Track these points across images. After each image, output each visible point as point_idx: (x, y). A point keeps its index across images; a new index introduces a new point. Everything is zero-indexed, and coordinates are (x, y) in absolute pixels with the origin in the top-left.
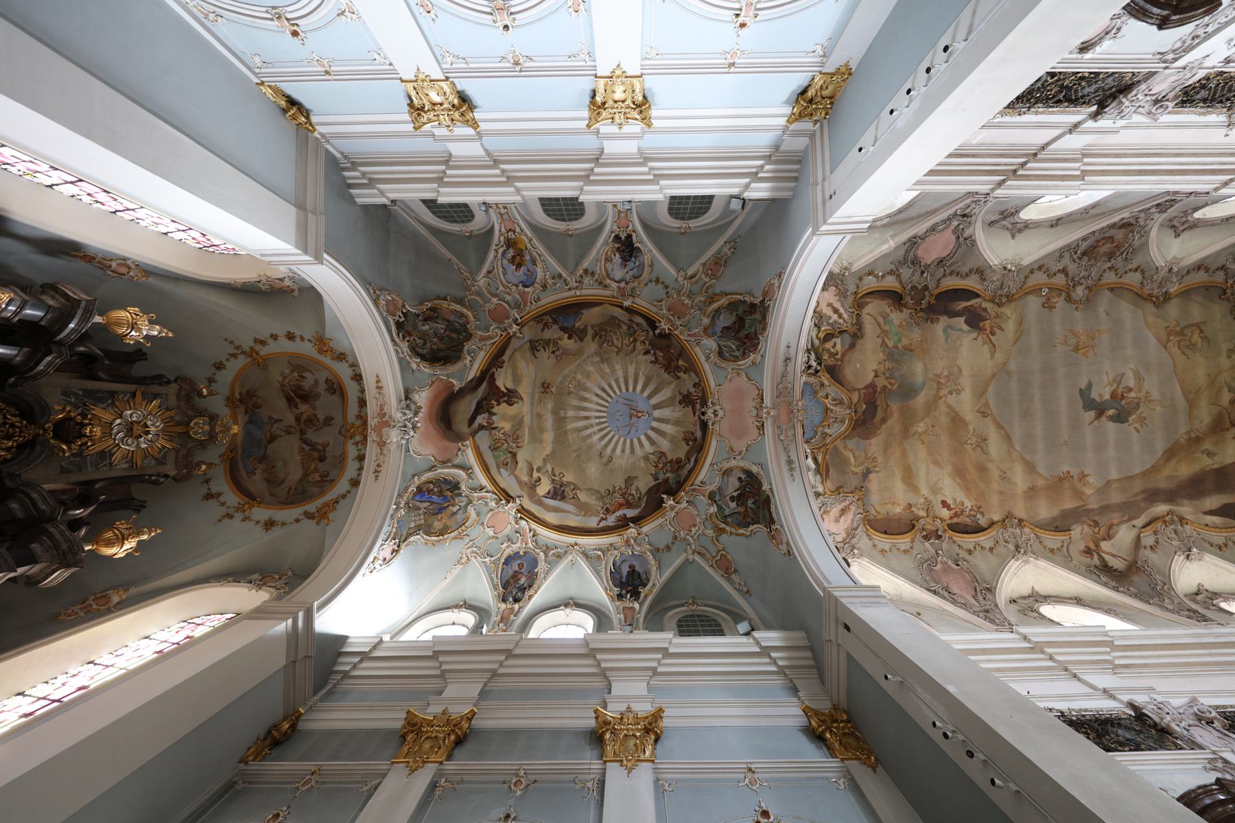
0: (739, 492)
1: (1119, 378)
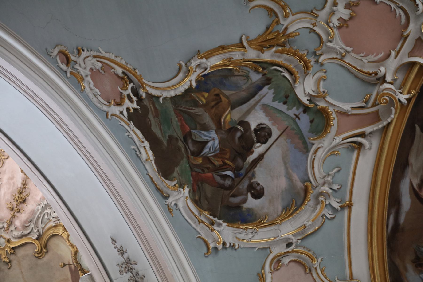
0: (251, 158)
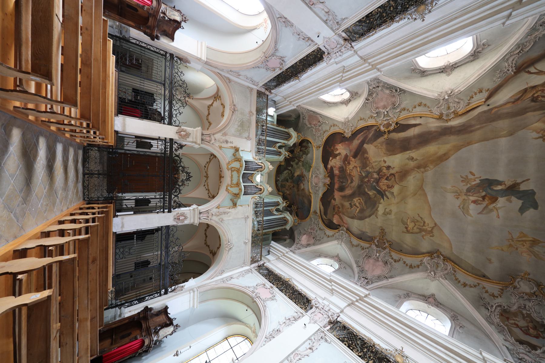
1: (485, 212)
